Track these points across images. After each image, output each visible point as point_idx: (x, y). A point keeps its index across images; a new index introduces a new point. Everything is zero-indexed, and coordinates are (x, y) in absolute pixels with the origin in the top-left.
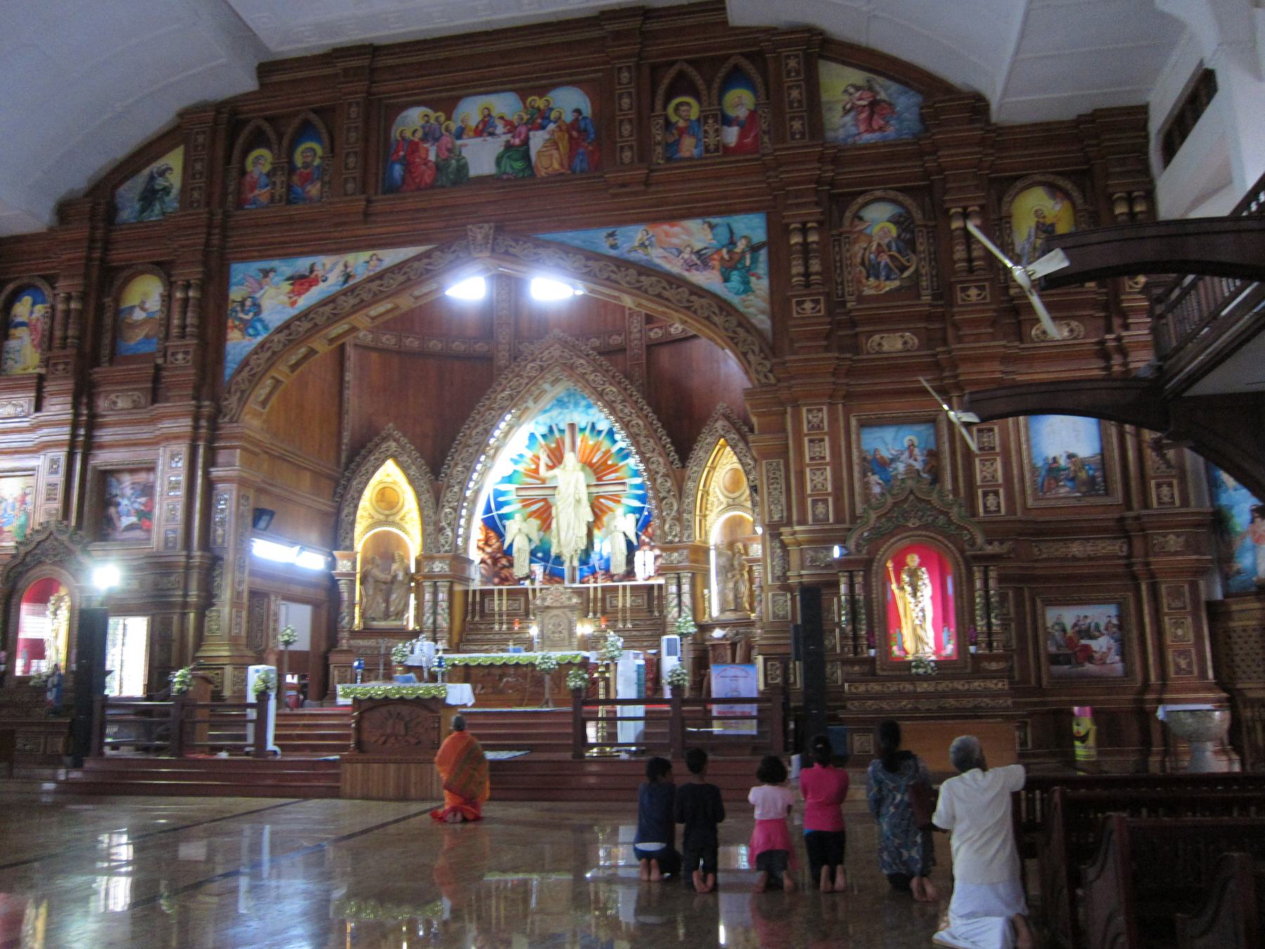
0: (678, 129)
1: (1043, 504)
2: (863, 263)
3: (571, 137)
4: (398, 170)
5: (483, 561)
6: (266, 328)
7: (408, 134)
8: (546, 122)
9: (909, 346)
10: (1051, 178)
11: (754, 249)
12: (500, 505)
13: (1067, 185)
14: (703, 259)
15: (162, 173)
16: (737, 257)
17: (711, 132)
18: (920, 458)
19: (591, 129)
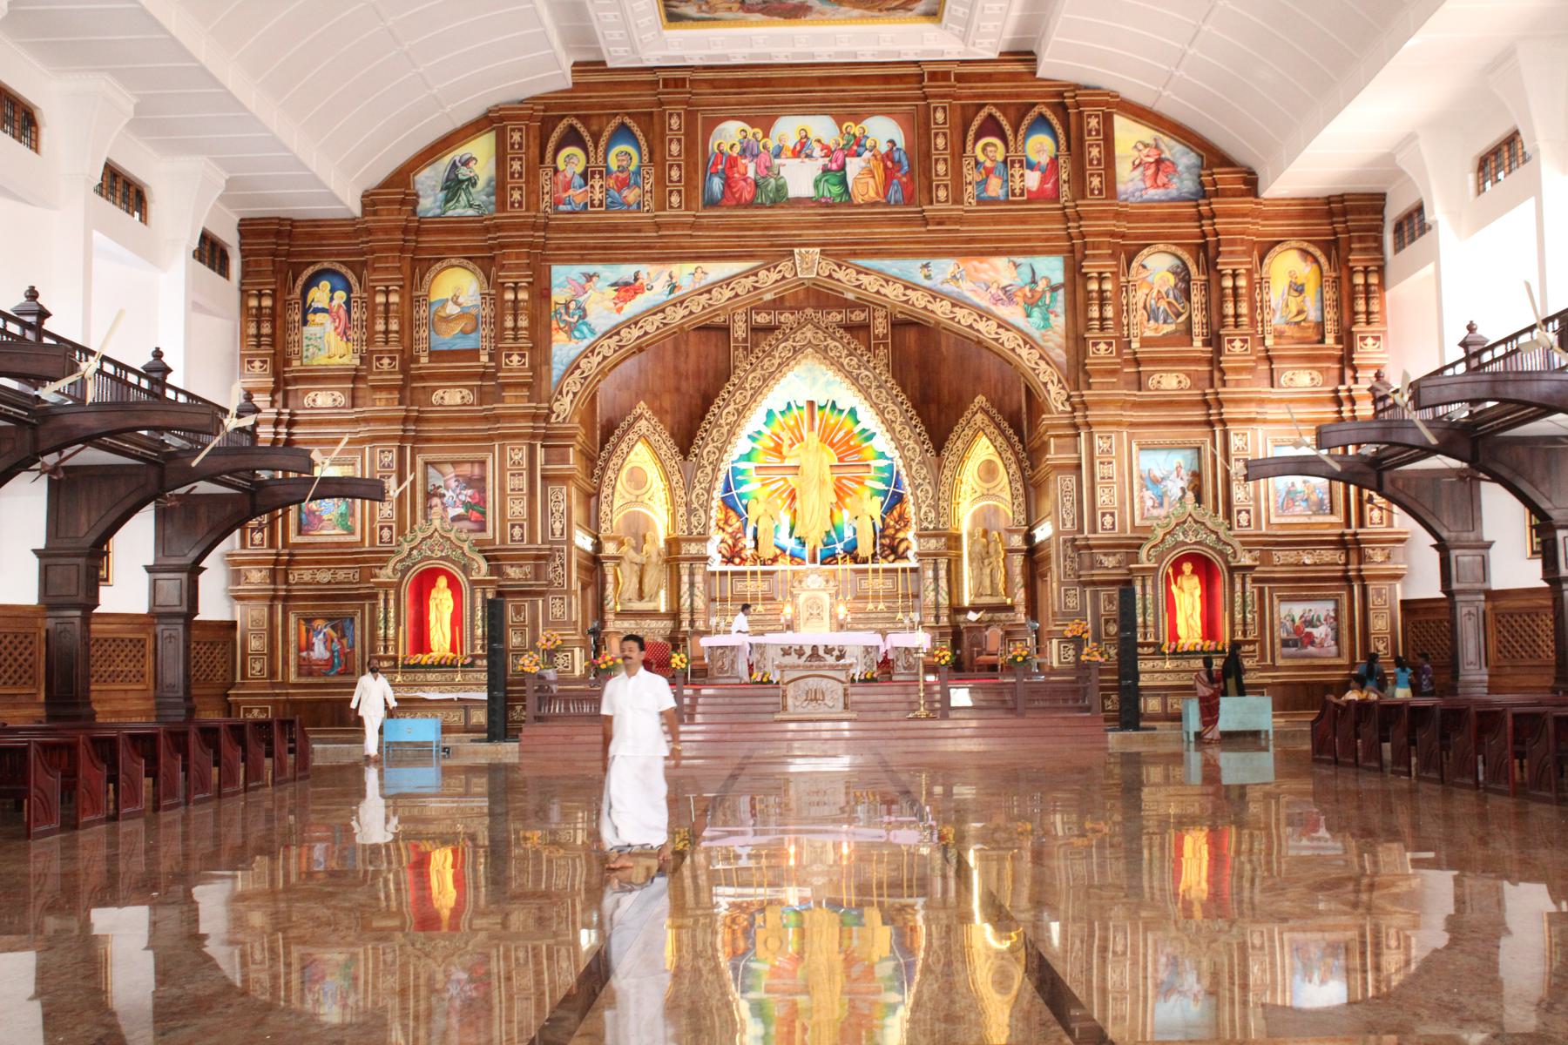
1: (1283, 520)
3: (886, 167)
4: (717, 184)
5: (723, 541)
6: (592, 332)
7: (726, 148)
10: (1305, 245)
11: (1054, 289)
12: (739, 484)
13: (1318, 253)
14: (1008, 295)
15: (466, 163)
16: (1037, 295)
17: (1017, 176)
18: (1186, 478)
19: (905, 162)
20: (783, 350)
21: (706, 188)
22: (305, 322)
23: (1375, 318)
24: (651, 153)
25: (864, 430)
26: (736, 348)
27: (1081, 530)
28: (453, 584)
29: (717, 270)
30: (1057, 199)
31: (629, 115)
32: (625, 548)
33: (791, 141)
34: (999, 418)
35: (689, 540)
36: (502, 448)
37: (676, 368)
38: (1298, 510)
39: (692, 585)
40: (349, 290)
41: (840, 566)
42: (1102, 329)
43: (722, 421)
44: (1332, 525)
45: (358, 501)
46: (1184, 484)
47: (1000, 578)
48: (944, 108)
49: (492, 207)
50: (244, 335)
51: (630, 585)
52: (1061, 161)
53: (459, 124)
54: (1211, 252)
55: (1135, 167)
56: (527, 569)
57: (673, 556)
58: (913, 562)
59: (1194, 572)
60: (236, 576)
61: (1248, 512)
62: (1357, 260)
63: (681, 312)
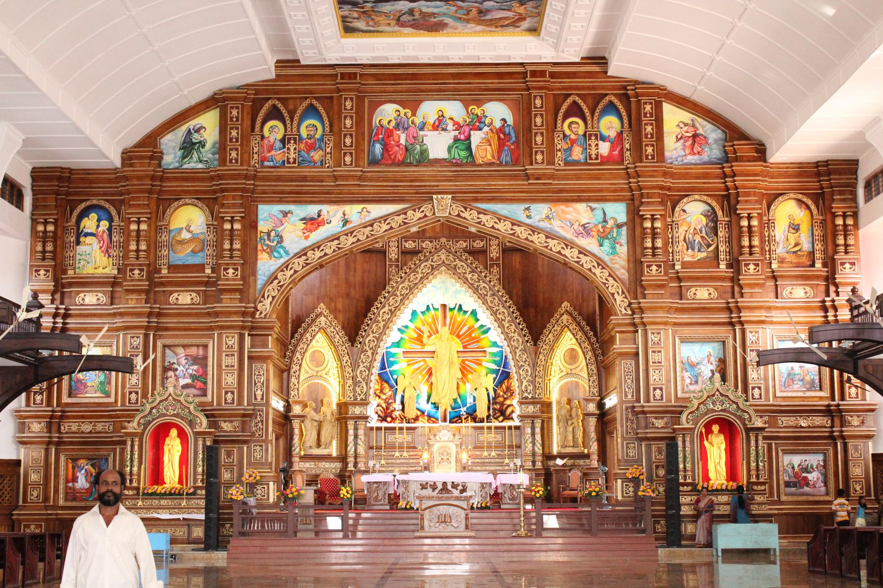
0: (570, 139)
1: (785, 394)
2: (685, 240)
3: (499, 138)
4: (378, 148)
5: (378, 406)
6: (287, 253)
7: (385, 123)
8: (482, 125)
9: (712, 296)
11: (619, 226)
12: (391, 364)
13: (810, 202)
14: (586, 230)
15: (198, 131)
16: (607, 231)
17: (593, 145)
18: (714, 363)
19: (513, 135)
20: (424, 268)
21: (371, 152)
22: (78, 243)
23: (850, 249)
24: (331, 125)
25: (482, 326)
26: (390, 266)
27: (638, 400)
28: (182, 435)
29: (378, 210)
30: (621, 162)
31: (315, 98)
32: (308, 410)
33: (432, 118)
34: (579, 318)
35: (354, 404)
36: (220, 335)
37: (347, 279)
38: (796, 387)
39: (356, 436)
40: (111, 220)
41: (463, 425)
42: (654, 255)
43: (380, 319)
44: (821, 398)
45: (114, 373)
46: (713, 367)
47: (580, 435)
48: (541, 97)
49: (216, 163)
50: (33, 251)
51: (311, 436)
52: (625, 135)
53: (193, 103)
54: (733, 201)
55: (678, 139)
56: (236, 424)
57: (342, 416)
58: (516, 422)
59: (720, 431)
60: (22, 427)
61: (760, 388)
62: (838, 207)
63: (351, 240)
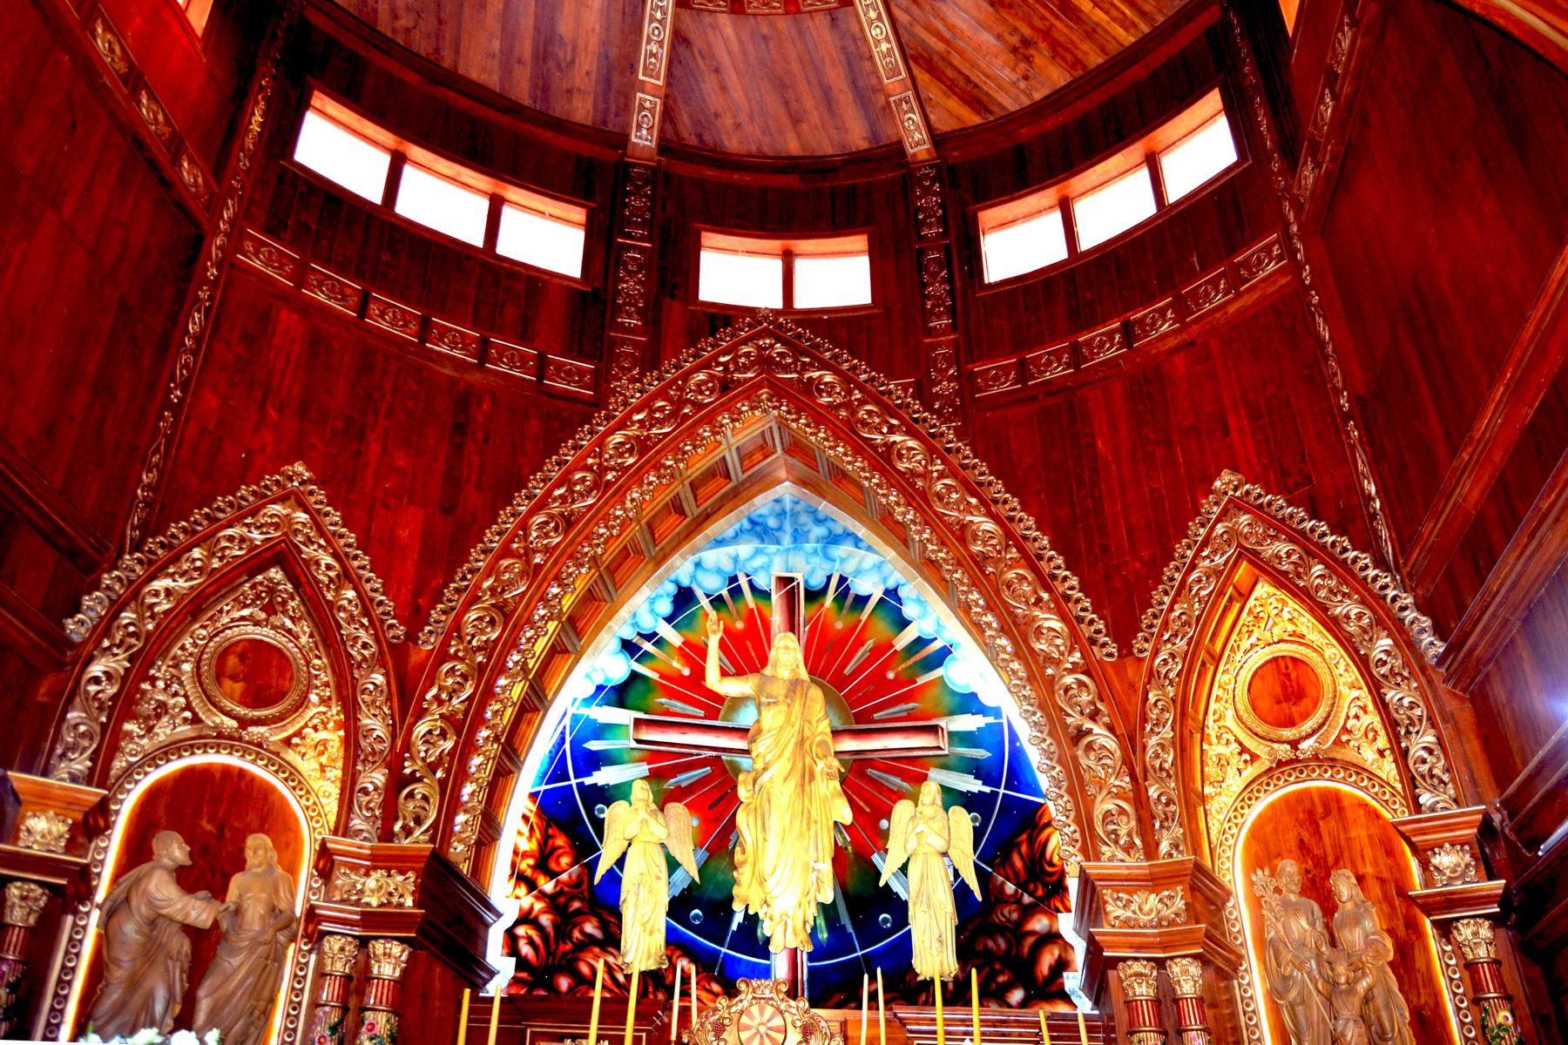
5: (526, 918)
